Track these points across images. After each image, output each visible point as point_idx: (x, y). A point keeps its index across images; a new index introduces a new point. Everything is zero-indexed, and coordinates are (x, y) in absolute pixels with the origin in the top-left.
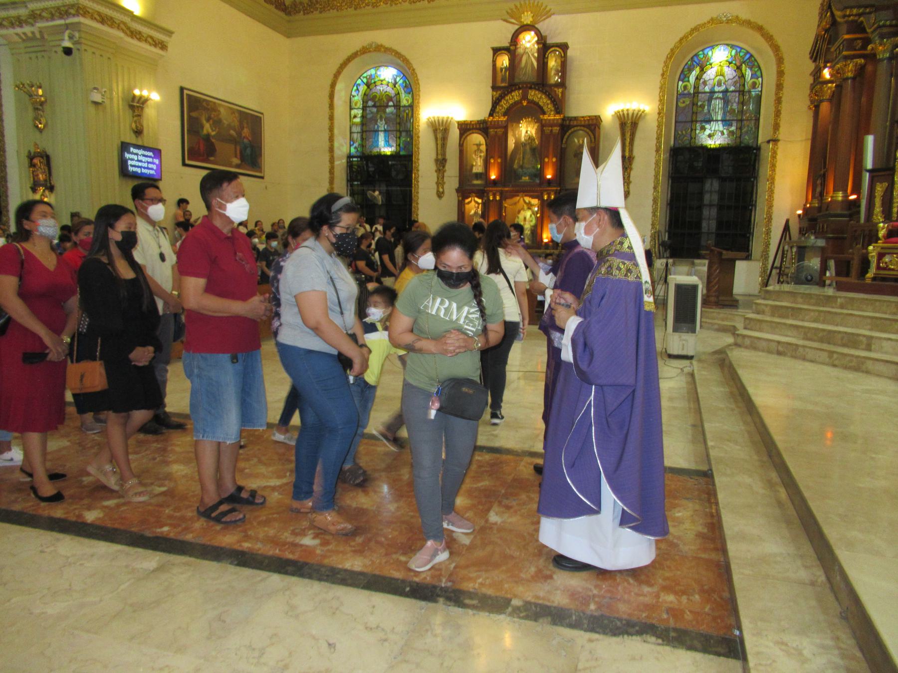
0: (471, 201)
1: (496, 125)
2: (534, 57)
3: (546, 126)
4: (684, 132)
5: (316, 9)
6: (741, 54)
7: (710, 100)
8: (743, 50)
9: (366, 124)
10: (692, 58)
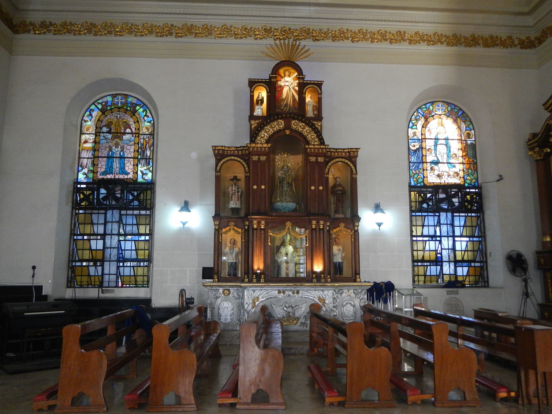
0: (230, 230)
1: (259, 154)
2: (295, 90)
3: (311, 156)
4: (417, 171)
5: (49, 31)
6: (456, 110)
7: (436, 145)
8: (456, 108)
9: (98, 150)
10: (417, 110)
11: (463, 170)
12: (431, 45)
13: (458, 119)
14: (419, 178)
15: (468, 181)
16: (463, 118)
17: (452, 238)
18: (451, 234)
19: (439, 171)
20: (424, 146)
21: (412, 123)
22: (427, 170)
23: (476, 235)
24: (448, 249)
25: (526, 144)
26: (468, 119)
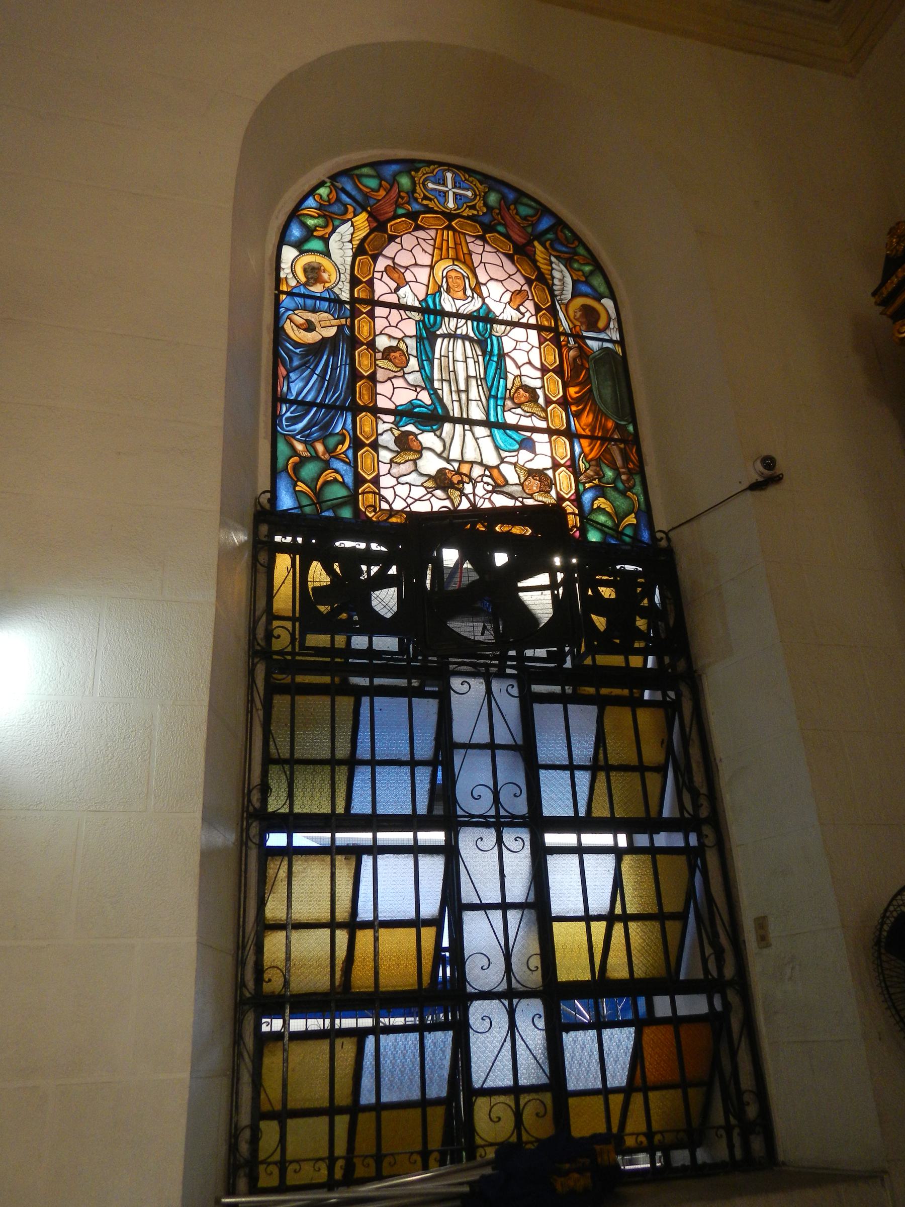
4: (320, 448)
6: (524, 211)
8: (525, 200)
10: (334, 178)
11: (572, 466)
13: (536, 243)
14: (326, 483)
18: (521, 807)
19: (448, 461)
20: (363, 333)
21: (304, 225)
23: (666, 814)
24: (504, 906)
25: (873, 300)
26: (581, 250)
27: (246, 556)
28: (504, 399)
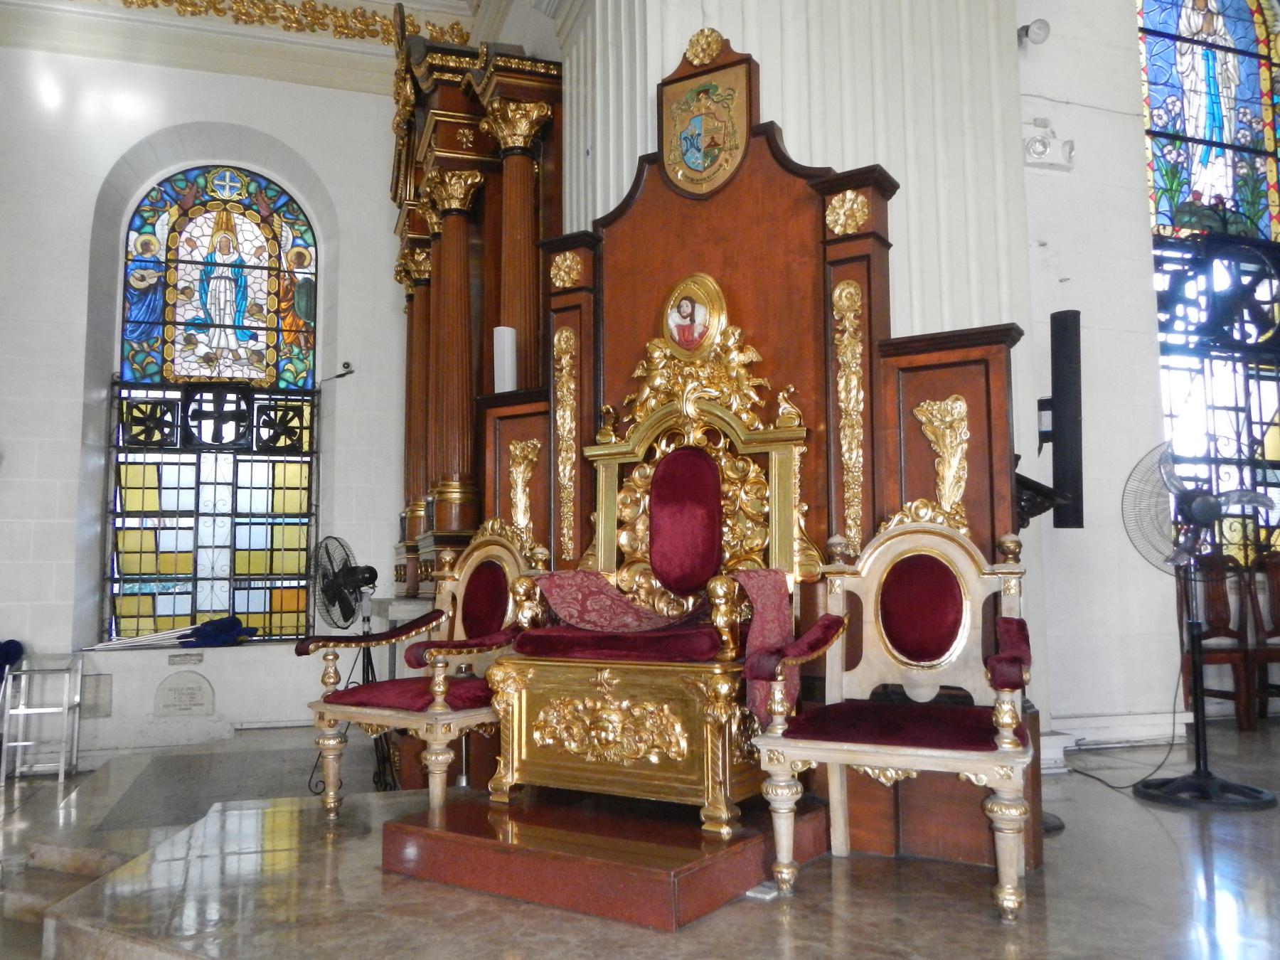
4: (145, 345)
6: (270, 193)
7: (205, 279)
11: (277, 347)
12: (188, 15)
14: (148, 363)
15: (288, 376)
16: (290, 213)
17: (228, 520)
19: (211, 348)
20: (171, 281)
21: (142, 217)
22: (173, 343)
26: (302, 217)
27: (105, 405)
28: (244, 312)
